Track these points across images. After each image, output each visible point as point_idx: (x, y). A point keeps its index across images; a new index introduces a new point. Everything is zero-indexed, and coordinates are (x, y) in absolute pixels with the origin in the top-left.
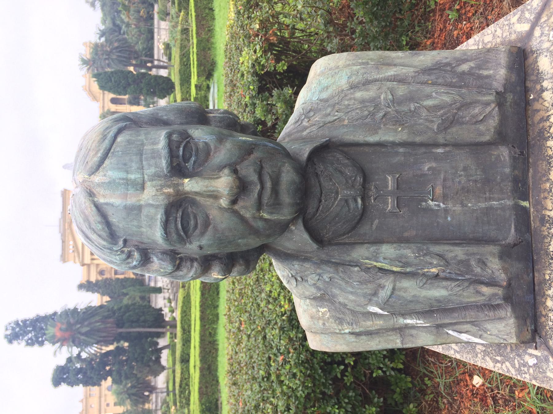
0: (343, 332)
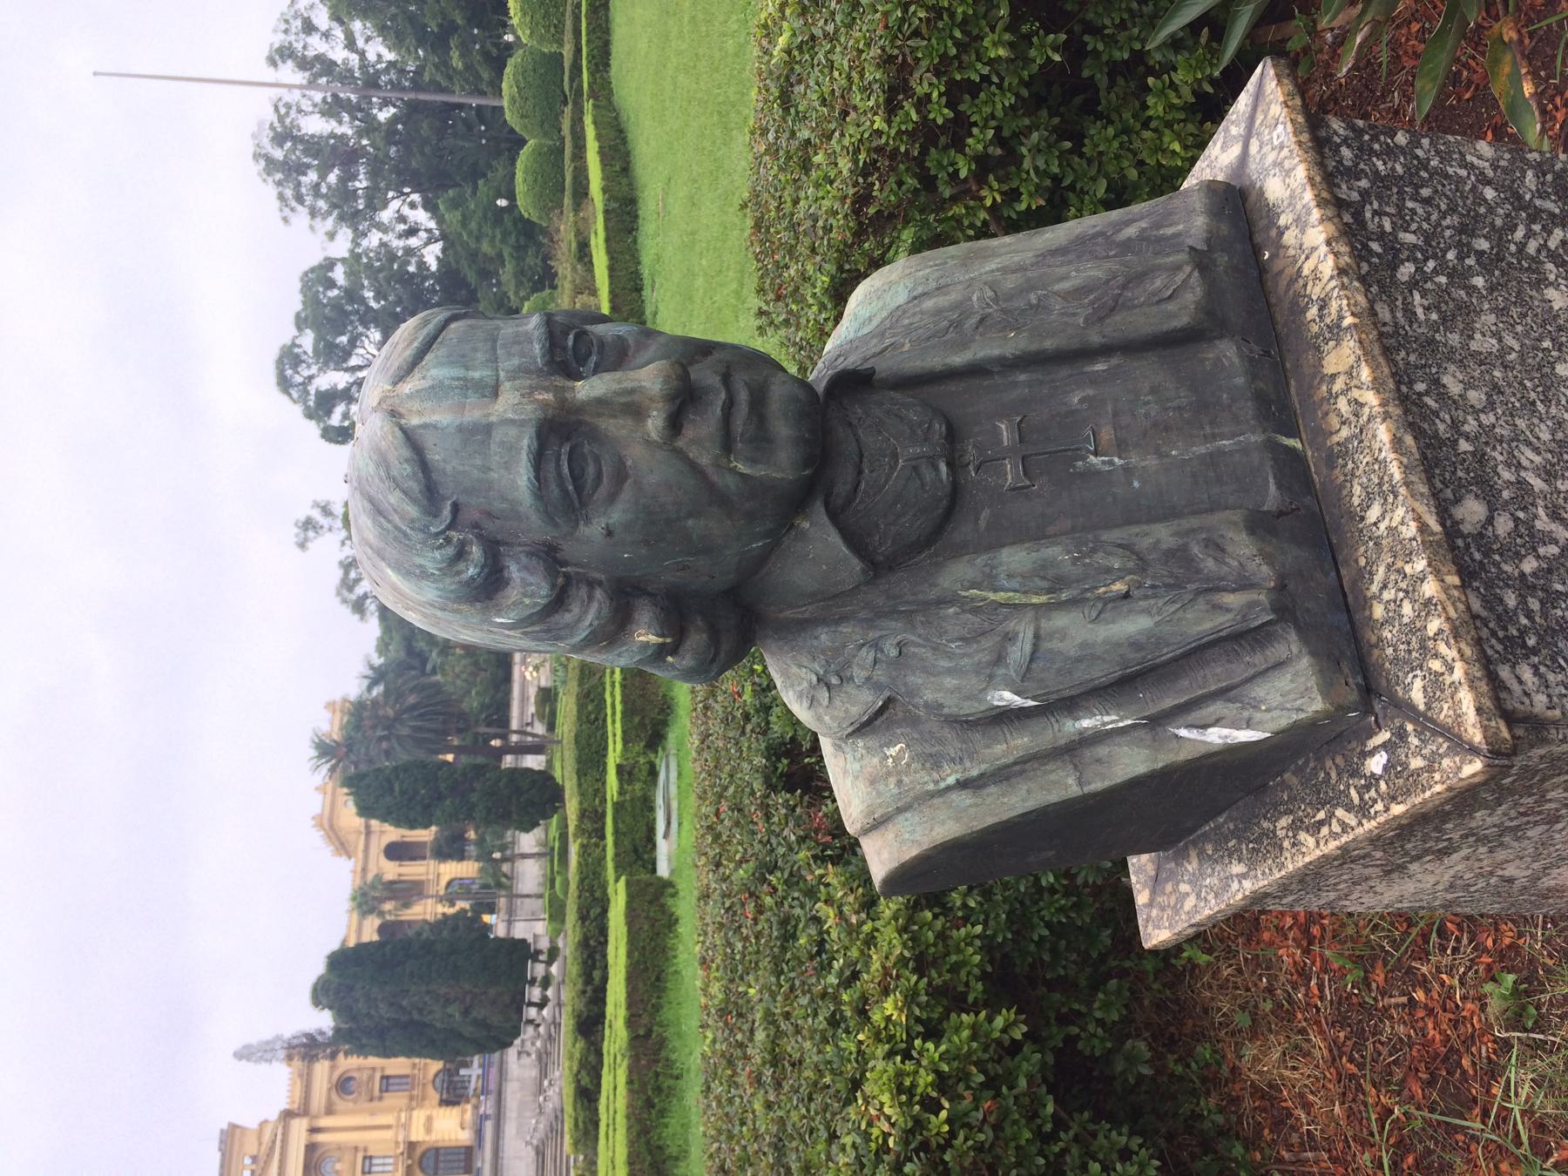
0: (943, 785)
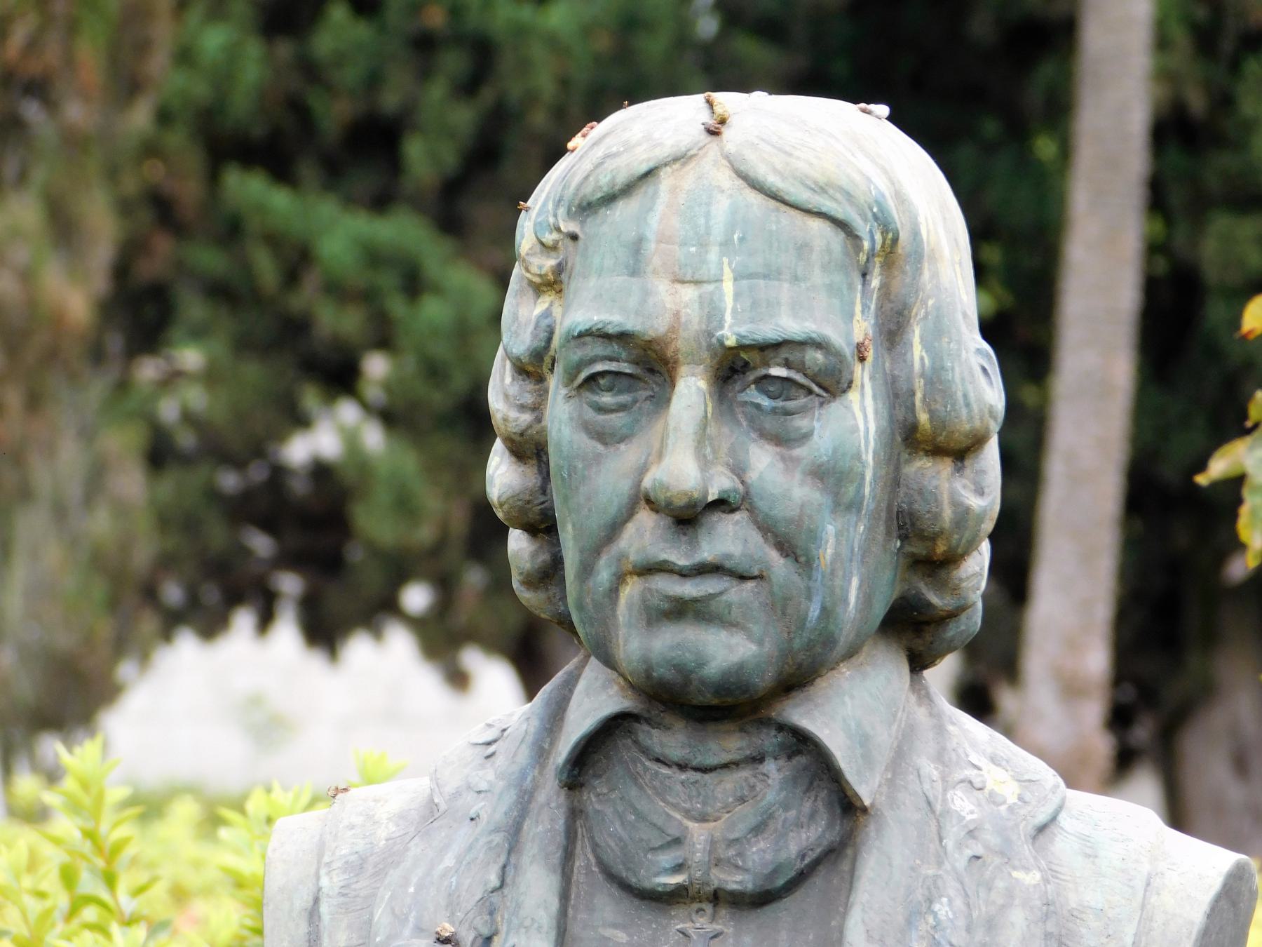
0: (323, 872)
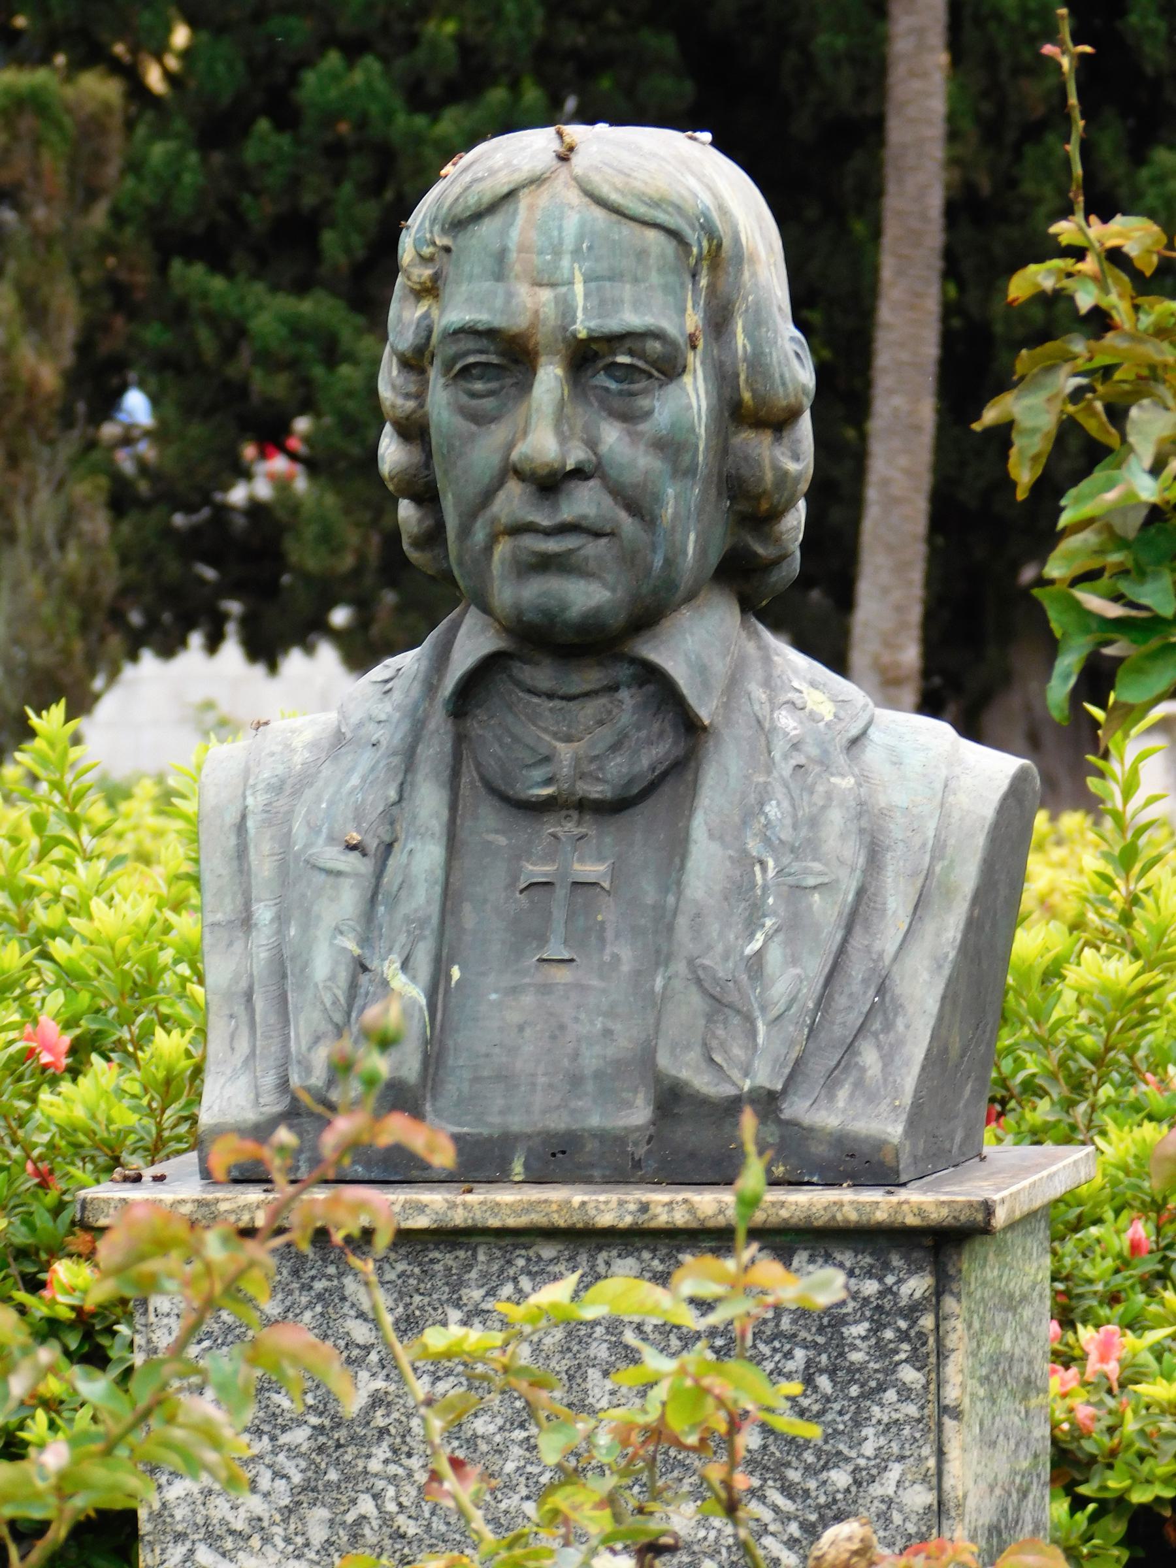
0: (248, 793)
